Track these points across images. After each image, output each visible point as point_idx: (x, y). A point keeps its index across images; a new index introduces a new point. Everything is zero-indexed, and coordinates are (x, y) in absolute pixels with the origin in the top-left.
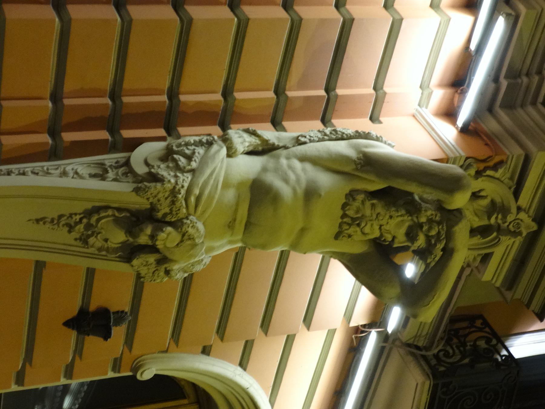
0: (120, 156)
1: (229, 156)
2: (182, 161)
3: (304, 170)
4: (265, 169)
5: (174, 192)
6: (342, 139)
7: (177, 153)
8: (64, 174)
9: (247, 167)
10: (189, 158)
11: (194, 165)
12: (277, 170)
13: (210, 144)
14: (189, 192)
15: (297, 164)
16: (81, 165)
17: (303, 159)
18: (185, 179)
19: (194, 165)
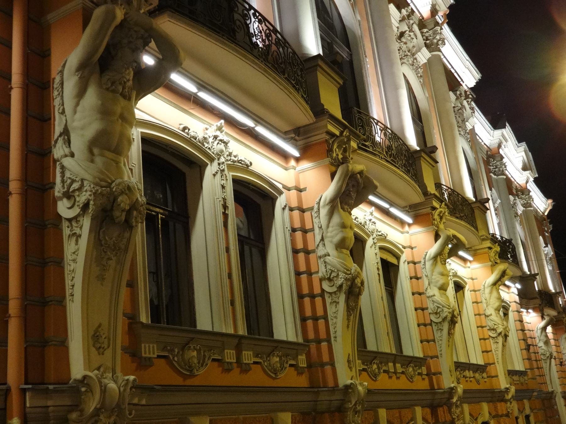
0: (326, 296)
1: (329, 255)
2: (334, 274)
3: (332, 227)
4: (331, 242)
5: (346, 279)
6: (319, 209)
7: (330, 275)
8: (336, 317)
9: (330, 248)
10: (332, 271)
11: (336, 270)
12: (332, 237)
13: (325, 262)
14: (346, 274)
15: (330, 229)
16: (331, 310)
17: (328, 227)
18: (341, 275)
19: (336, 270)
